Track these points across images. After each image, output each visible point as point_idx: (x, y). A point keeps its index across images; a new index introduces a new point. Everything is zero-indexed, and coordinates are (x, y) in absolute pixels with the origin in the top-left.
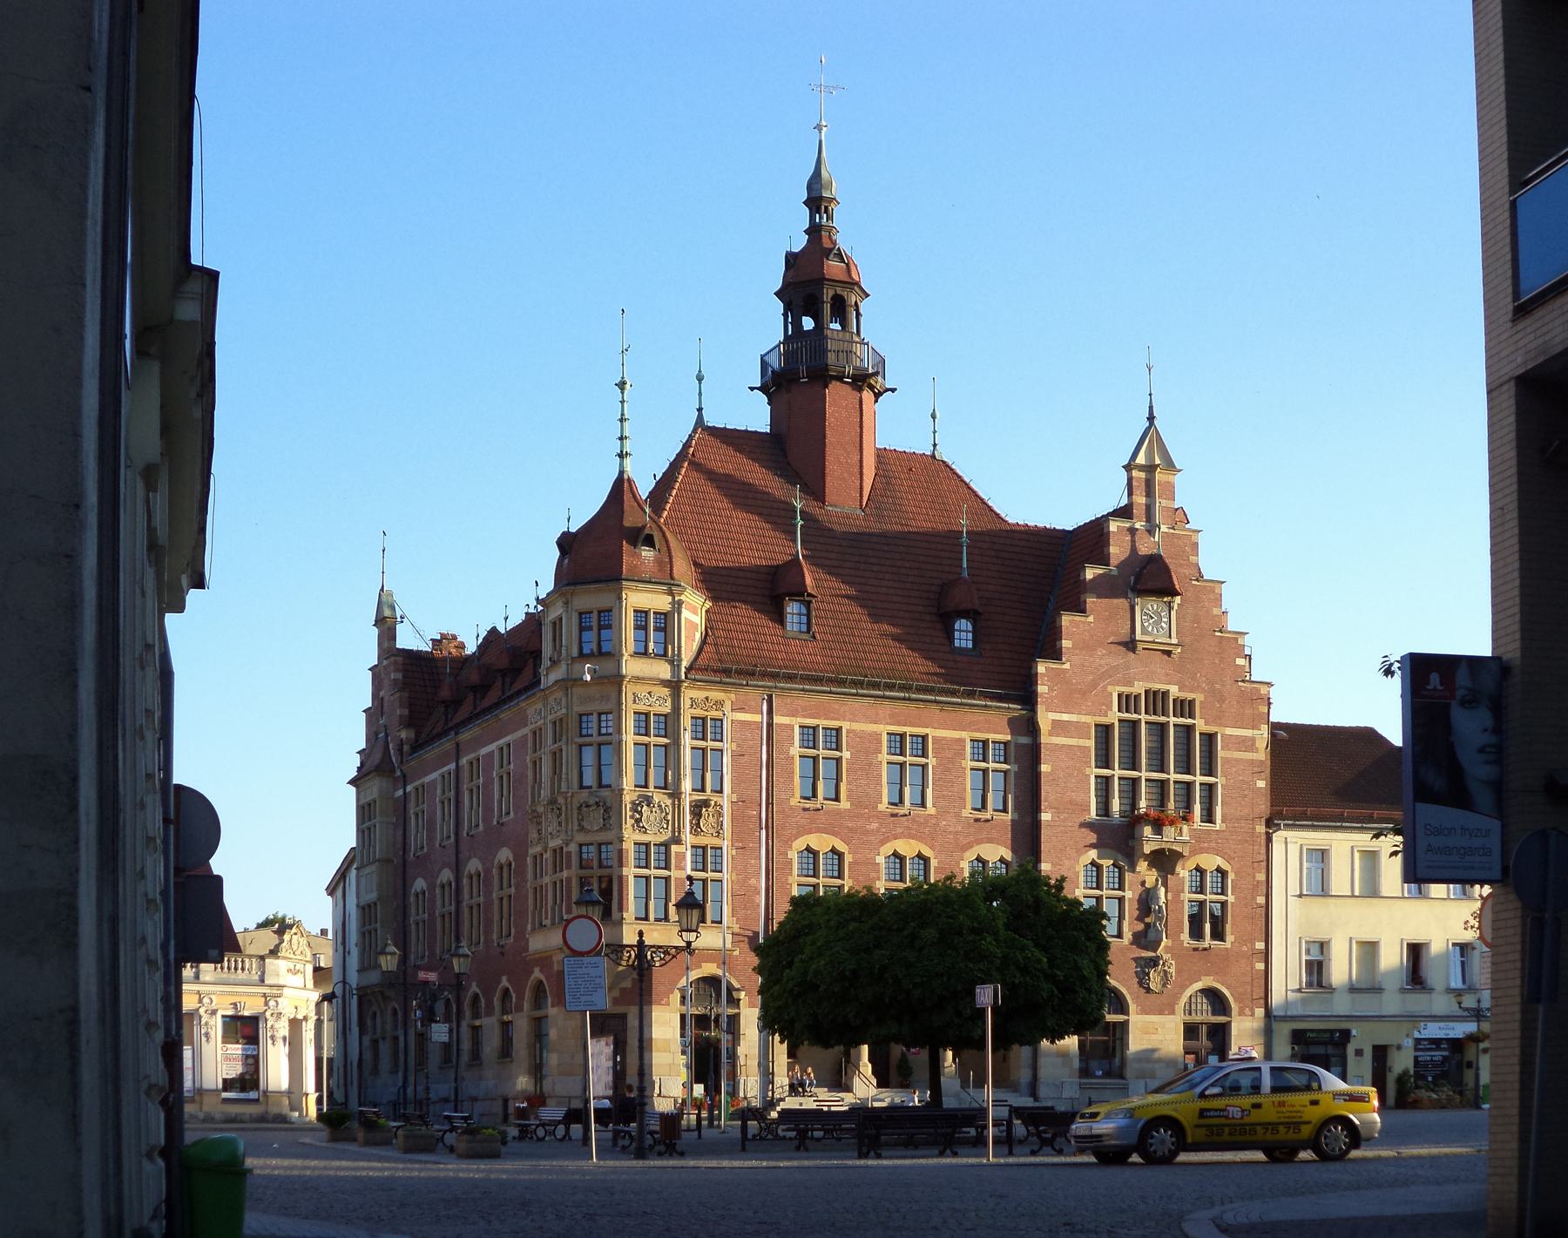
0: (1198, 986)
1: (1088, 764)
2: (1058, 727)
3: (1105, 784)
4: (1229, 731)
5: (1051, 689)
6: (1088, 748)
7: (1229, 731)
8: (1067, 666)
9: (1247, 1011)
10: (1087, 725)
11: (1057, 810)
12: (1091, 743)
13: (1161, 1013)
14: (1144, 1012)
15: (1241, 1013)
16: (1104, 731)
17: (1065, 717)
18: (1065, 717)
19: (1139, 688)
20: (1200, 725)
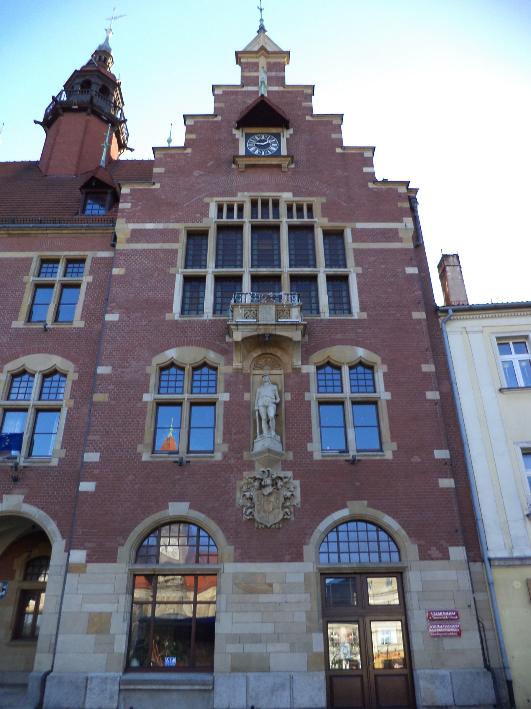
0: (343, 513)
1: (173, 264)
2: (136, 236)
3: (194, 283)
4: (360, 225)
5: (134, 205)
6: (175, 251)
7: (360, 225)
8: (157, 186)
9: (434, 551)
10: (176, 232)
11: (124, 308)
12: (180, 246)
13: (278, 558)
14: (244, 556)
15: (424, 556)
16: (197, 237)
17: (149, 226)
18: (149, 226)
19: (243, 197)
20: (321, 222)
